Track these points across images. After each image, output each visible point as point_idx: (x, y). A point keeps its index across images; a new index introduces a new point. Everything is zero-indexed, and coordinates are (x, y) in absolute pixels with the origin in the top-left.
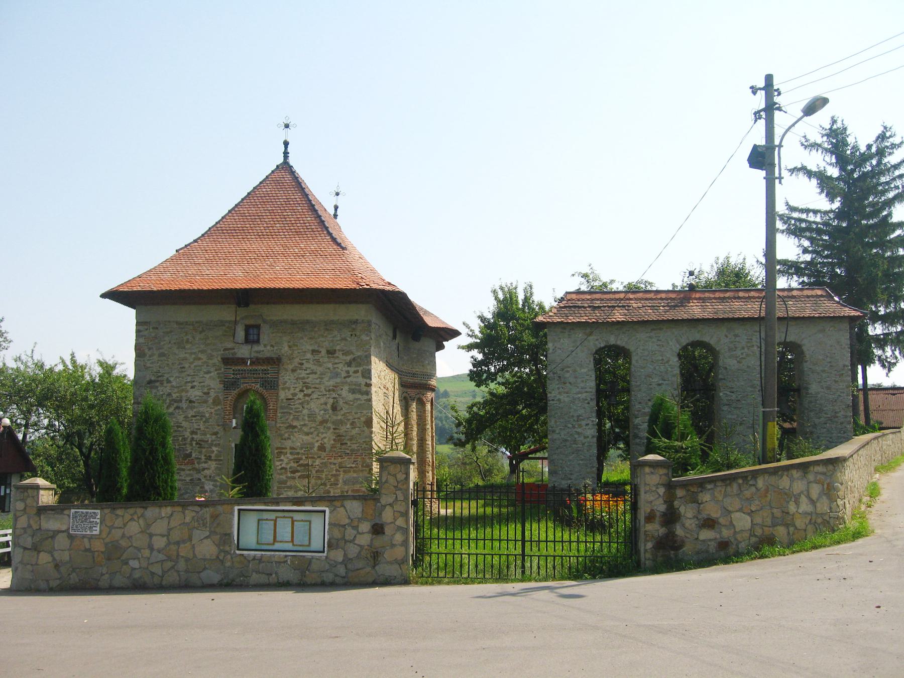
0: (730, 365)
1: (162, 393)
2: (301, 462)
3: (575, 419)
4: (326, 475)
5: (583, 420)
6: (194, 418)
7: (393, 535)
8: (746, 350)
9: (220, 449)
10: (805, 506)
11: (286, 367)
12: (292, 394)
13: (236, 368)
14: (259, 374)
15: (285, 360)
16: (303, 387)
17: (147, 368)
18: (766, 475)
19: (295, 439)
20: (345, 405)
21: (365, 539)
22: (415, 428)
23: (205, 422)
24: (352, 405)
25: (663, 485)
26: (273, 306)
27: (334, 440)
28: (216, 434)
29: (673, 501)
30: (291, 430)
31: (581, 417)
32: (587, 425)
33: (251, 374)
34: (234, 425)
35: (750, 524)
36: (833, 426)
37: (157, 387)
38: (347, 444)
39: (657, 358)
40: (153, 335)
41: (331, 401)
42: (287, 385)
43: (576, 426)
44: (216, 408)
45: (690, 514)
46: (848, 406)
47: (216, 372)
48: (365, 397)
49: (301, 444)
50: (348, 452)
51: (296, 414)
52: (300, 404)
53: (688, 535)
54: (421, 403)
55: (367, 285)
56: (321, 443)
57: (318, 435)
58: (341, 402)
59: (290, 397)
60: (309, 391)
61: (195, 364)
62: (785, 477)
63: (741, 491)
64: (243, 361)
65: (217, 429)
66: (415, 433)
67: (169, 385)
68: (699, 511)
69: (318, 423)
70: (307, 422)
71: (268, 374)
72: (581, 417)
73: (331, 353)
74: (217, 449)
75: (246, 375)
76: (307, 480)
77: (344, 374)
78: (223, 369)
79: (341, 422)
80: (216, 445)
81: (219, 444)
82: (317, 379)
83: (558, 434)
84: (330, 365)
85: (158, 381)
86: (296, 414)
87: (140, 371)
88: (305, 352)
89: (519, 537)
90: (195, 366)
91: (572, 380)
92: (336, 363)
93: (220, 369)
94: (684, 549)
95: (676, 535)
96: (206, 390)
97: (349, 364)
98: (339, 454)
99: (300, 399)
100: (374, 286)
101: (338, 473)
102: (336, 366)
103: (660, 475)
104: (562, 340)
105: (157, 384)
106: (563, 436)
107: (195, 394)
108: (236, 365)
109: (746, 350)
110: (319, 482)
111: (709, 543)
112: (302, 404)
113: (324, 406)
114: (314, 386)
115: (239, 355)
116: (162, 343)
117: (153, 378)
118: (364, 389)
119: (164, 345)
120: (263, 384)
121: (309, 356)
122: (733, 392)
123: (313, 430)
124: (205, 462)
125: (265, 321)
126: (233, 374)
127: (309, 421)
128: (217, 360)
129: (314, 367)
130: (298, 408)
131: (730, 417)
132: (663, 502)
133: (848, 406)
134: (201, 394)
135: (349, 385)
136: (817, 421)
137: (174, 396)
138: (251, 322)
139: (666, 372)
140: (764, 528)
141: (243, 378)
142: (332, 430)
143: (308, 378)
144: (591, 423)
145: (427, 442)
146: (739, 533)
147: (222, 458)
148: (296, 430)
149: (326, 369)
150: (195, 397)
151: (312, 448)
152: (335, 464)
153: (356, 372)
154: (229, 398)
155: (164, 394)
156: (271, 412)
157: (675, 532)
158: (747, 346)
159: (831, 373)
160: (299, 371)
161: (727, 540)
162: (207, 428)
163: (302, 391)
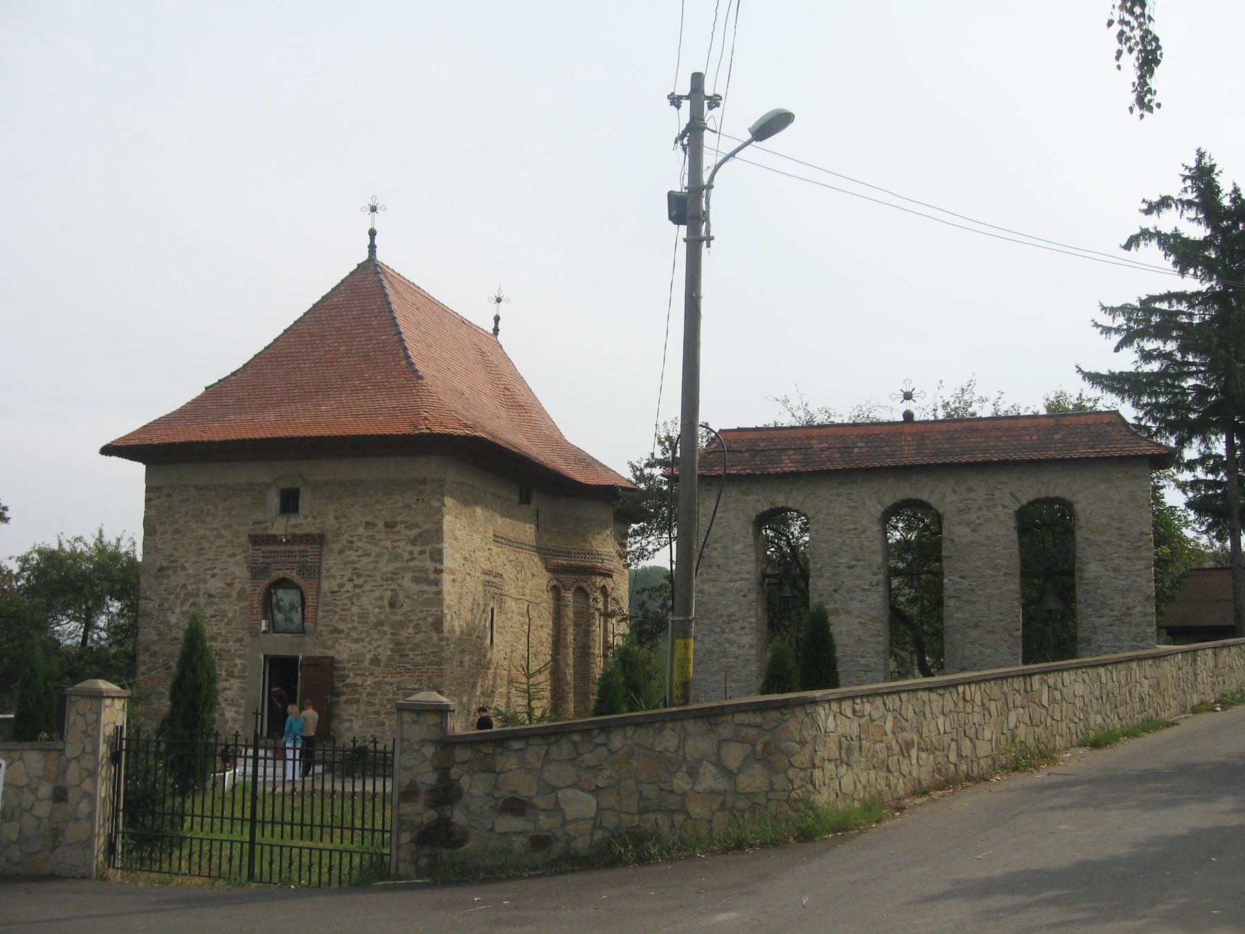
0: (959, 536)
1: (175, 584)
2: (348, 681)
3: (725, 619)
4: (380, 700)
5: (736, 621)
6: (213, 619)
7: (78, 804)
8: (985, 511)
9: (245, 662)
10: (709, 779)
11: (331, 546)
14: (296, 556)
15: (329, 536)
16: (352, 574)
17: (157, 550)
18: (628, 728)
19: (340, 648)
20: (407, 600)
21: (44, 809)
22: (571, 630)
23: (227, 624)
24: (416, 600)
25: (434, 742)
27: (392, 650)
28: (240, 640)
29: (449, 768)
30: (336, 635)
31: (734, 618)
32: (743, 628)
34: (263, 628)
35: (595, 811)
36: (1125, 629)
37: (169, 577)
38: (408, 655)
39: (847, 528)
40: (166, 504)
41: (389, 594)
42: (332, 572)
43: (727, 631)
44: (241, 605)
45: (477, 791)
46: (1149, 598)
47: (242, 555)
48: (434, 589)
49: (349, 656)
50: (409, 666)
51: (343, 613)
52: (349, 598)
53: (473, 823)
54: (582, 592)
55: (428, 428)
56: (375, 655)
57: (371, 644)
58: (401, 596)
59: (336, 588)
60: (361, 581)
61: (217, 544)
62: (667, 733)
63: (579, 754)
64: (274, 539)
65: (242, 634)
66: (570, 638)
67: (184, 573)
68: (495, 786)
69: (371, 626)
70: (356, 624)
71: (307, 556)
72: (734, 618)
73: (389, 525)
74: (241, 661)
76: (355, 706)
77: (406, 556)
78: (251, 551)
79: (401, 625)
80: (240, 657)
81: (244, 655)
82: (371, 563)
83: (700, 642)
84: (389, 544)
85: (170, 568)
86: (343, 613)
87: (149, 553)
88: (356, 525)
89: (248, 815)
90: (218, 547)
91: (721, 561)
92: (397, 541)
93: (248, 551)
94: (467, 846)
95: (453, 823)
96: (229, 581)
97: (413, 542)
98: (398, 670)
99: (347, 592)
100: (437, 429)
101: (396, 697)
102: (395, 544)
103: (428, 726)
104: (706, 502)
105: (170, 572)
106: (707, 646)
107: (215, 585)
109: (985, 511)
110: (372, 709)
111: (514, 839)
112: (350, 598)
113: (380, 602)
114: (367, 573)
115: (273, 532)
116: (178, 516)
117: (165, 564)
118: (432, 576)
119: (180, 518)
120: (300, 571)
121: (361, 530)
122: (963, 578)
123: (364, 635)
124: (226, 680)
126: (263, 557)
127: (359, 623)
128: (244, 539)
129: (367, 547)
130: (347, 605)
131: (959, 615)
132: (431, 769)
133: (1149, 598)
134: (221, 585)
135: (413, 571)
136: (1096, 621)
137: (190, 587)
138: (288, 484)
139: (861, 548)
140: (622, 815)
141: (276, 563)
142: (389, 636)
143: (360, 561)
144: (748, 626)
145: (592, 651)
146: (573, 821)
147: (247, 674)
148: (343, 635)
149: (384, 548)
150: (216, 589)
151: (359, 662)
152: (391, 684)
153: (422, 553)
154: (258, 591)
155: (178, 586)
157: (450, 818)
158: (986, 506)
159: (1121, 546)
160: (348, 553)
161: (548, 834)
162: (230, 633)
163: (351, 580)
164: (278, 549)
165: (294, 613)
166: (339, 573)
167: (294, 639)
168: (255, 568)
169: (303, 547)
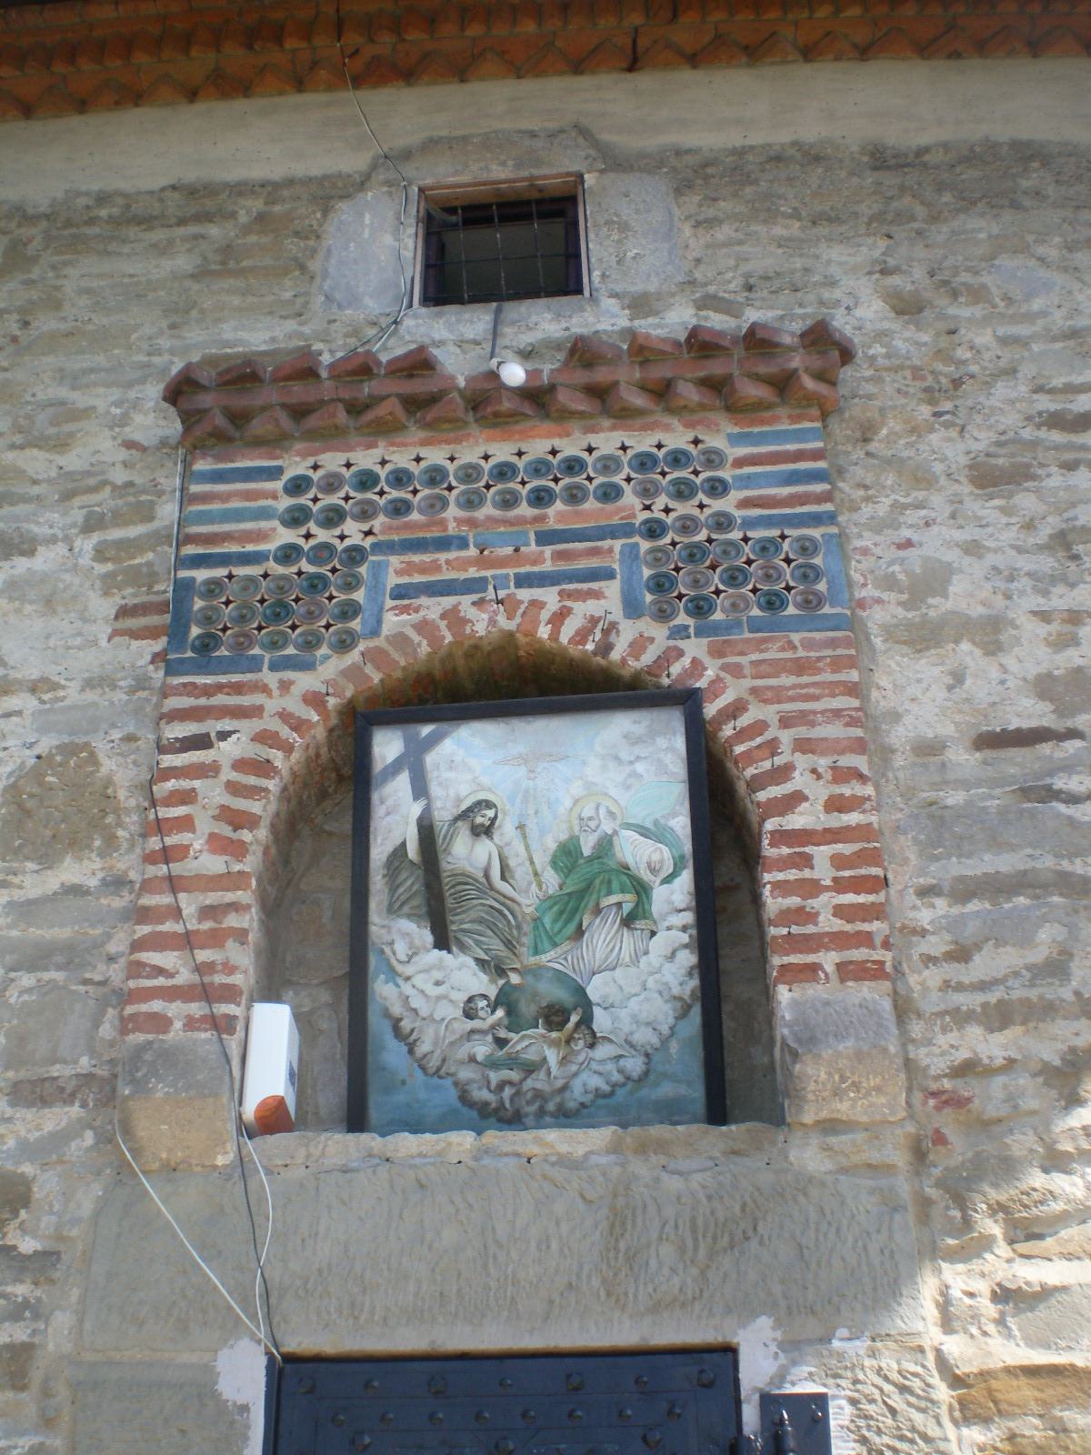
12: (1044, 686)
13: (332, 461)
14: (609, 494)
26: (687, 75)
33: (509, 501)
47: (87, 545)
59: (1029, 712)
75: (453, 512)
108: (331, 437)
125: (616, 163)
126: (296, 518)
154: (227, 751)
156: (823, 871)
164: (436, 456)
165: (603, 938)
166: (1037, 602)
167: (641, 1169)
168: (213, 588)
169: (677, 438)
